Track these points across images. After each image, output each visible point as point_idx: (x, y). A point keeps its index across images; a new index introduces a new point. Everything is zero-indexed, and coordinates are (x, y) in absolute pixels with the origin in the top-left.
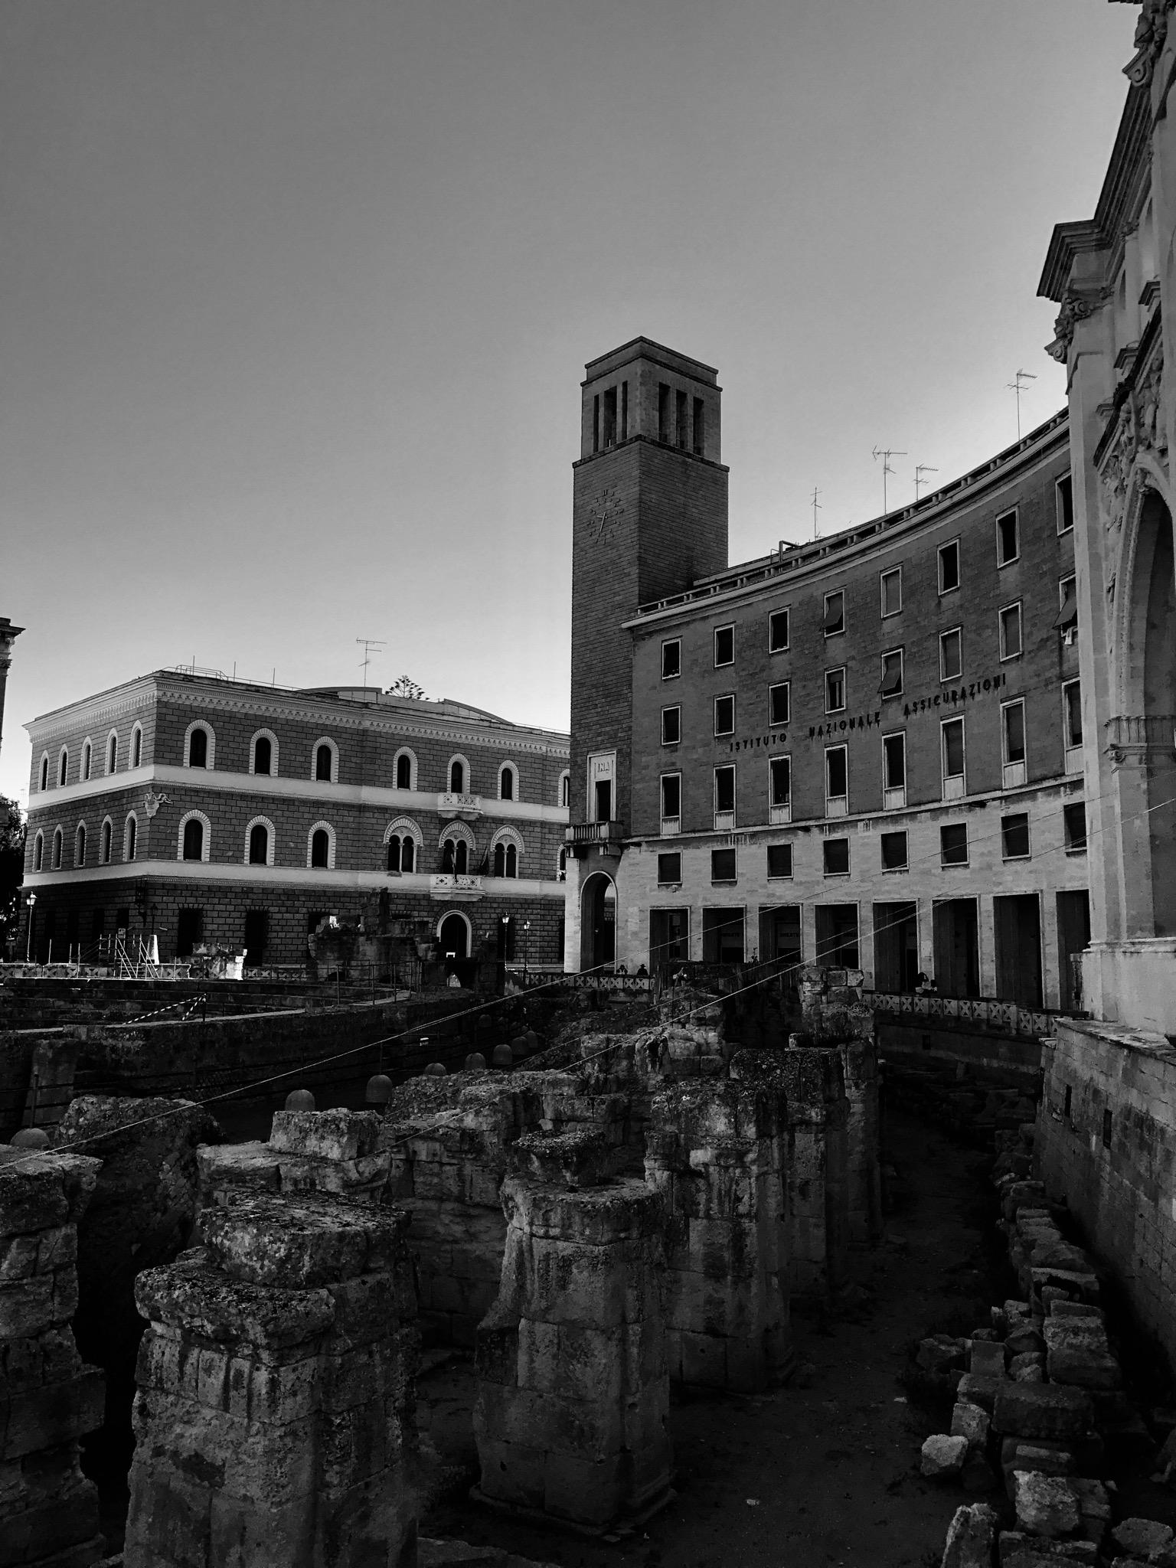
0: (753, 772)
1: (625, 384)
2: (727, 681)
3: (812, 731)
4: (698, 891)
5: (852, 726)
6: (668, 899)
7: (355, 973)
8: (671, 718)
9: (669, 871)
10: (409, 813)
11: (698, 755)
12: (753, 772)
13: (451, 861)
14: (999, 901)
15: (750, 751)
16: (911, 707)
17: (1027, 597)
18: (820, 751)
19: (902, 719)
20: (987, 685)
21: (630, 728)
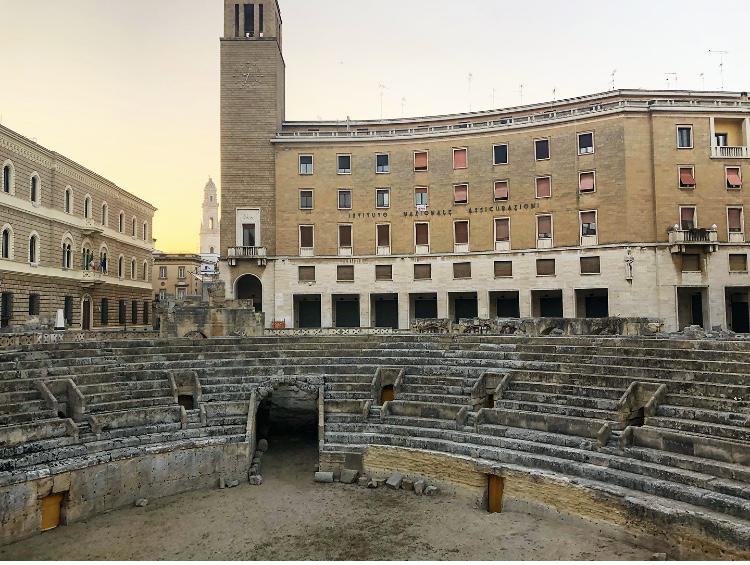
0: (364, 230)
1: (261, 6)
2: (347, 180)
3: (406, 214)
4: (326, 284)
5: (432, 213)
6: (305, 289)
7: (207, 330)
8: (307, 195)
9: (307, 273)
10: (71, 227)
11: (325, 218)
12: (364, 230)
13: (87, 261)
14: (534, 293)
15: (361, 219)
16: (473, 210)
17: (554, 175)
18: (410, 225)
19: (467, 214)
20: (526, 206)
21: (274, 196)
